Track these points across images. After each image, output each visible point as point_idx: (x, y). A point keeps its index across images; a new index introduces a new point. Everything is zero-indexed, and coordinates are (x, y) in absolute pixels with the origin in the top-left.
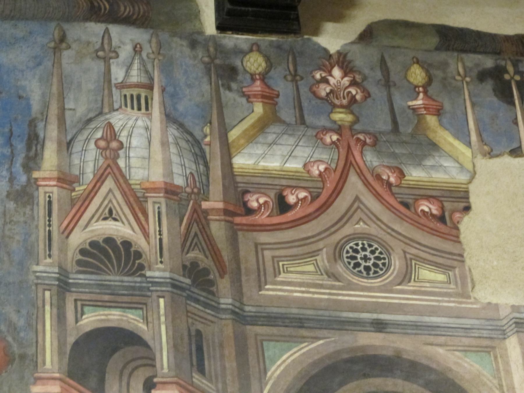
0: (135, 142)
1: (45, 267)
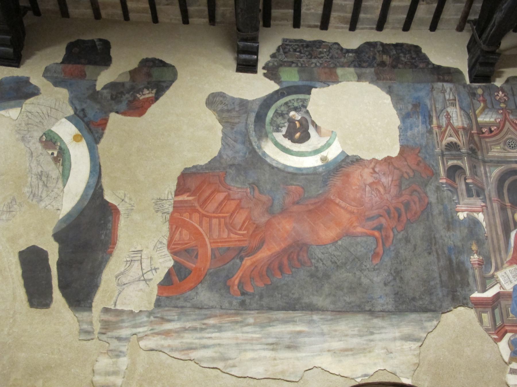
0: (454, 116)
1: (438, 150)
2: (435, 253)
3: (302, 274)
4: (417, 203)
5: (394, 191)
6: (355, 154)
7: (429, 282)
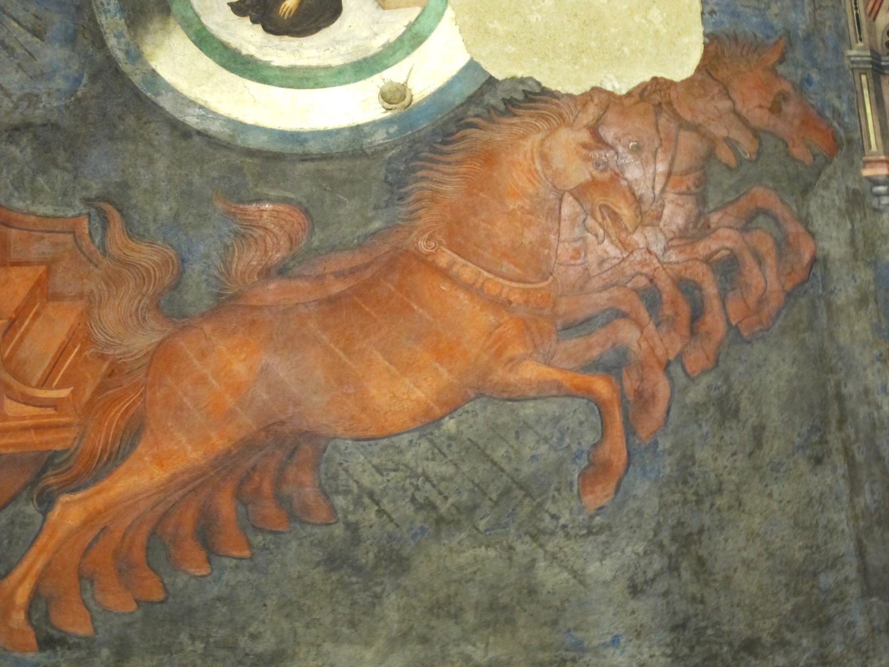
1: (857, 51)
2: (838, 459)
3: (295, 557)
4: (770, 261)
5: (675, 214)
6: (520, 74)
7: (815, 575)
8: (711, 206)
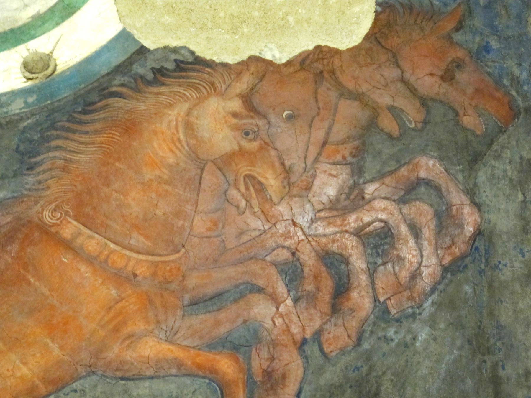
4: (427, 233)
5: (329, 186)
6: (174, 43)
8: (367, 176)
